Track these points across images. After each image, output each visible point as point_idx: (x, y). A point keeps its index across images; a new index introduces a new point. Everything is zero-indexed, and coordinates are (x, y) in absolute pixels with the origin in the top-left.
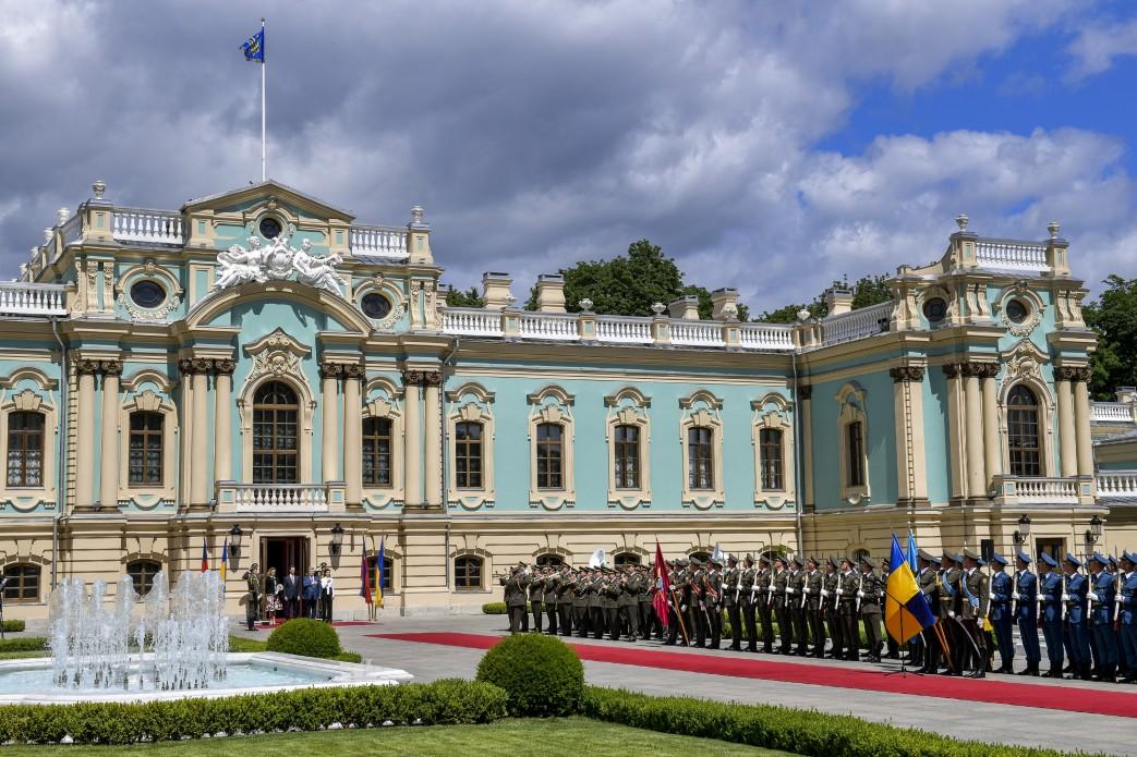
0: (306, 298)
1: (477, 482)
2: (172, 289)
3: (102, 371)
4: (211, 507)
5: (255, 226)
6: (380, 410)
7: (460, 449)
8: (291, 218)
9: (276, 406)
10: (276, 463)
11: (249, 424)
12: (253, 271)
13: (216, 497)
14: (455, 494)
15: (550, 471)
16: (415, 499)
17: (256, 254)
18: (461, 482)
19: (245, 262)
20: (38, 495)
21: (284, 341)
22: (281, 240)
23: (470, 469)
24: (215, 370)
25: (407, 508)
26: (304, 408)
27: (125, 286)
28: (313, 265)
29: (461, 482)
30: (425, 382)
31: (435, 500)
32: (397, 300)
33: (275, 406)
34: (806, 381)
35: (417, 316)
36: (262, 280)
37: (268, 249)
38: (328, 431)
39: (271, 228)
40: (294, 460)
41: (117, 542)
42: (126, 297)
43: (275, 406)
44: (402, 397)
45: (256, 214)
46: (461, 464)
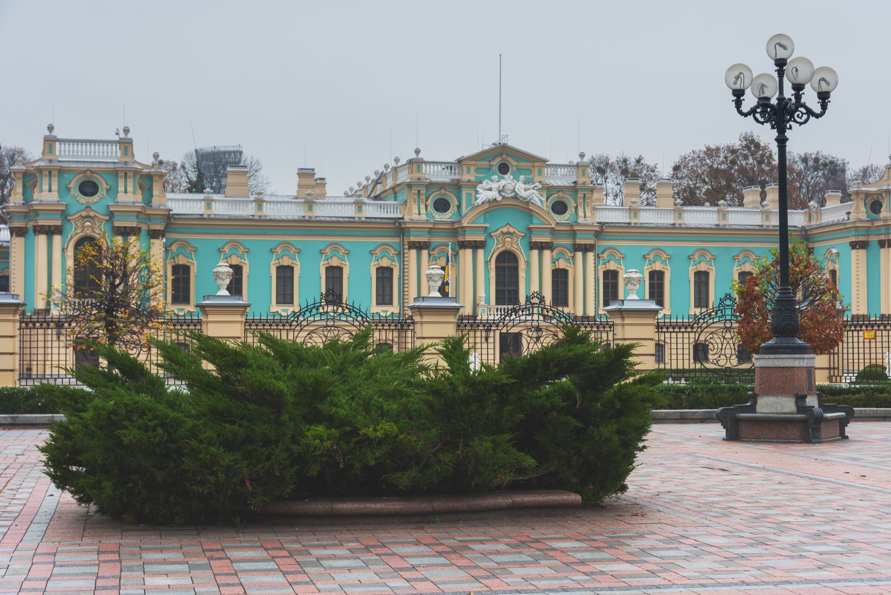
0: (524, 207)
2: (454, 202)
5: (495, 168)
6: (562, 264)
8: (516, 163)
11: (493, 274)
17: (495, 185)
19: (490, 189)
21: (511, 230)
22: (509, 177)
24: (476, 246)
26: (522, 265)
27: (430, 202)
28: (526, 190)
30: (586, 249)
32: (571, 205)
33: (506, 265)
35: (581, 214)
36: (499, 198)
37: (503, 182)
38: (535, 278)
39: (504, 169)
40: (516, 292)
42: (431, 209)
43: (506, 265)
44: (574, 257)
45: (496, 162)
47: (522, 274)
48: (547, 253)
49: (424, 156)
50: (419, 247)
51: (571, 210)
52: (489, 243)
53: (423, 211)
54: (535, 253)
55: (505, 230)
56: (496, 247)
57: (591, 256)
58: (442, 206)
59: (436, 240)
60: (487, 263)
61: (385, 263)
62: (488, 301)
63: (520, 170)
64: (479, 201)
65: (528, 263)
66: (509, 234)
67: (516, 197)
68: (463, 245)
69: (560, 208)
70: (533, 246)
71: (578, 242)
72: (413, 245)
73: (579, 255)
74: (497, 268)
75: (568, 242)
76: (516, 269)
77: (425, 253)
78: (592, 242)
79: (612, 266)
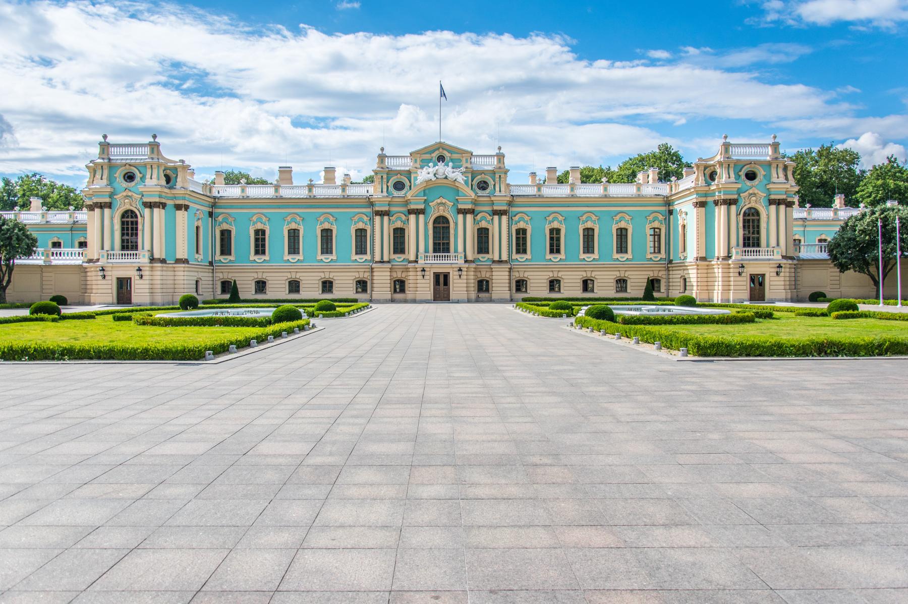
1: (525, 252)
3: (387, 213)
4: (416, 262)
5: (435, 159)
6: (484, 224)
7: (517, 238)
9: (441, 227)
10: (441, 245)
11: (431, 232)
12: (431, 176)
13: (417, 257)
14: (515, 256)
15: (555, 248)
16: (496, 258)
17: (430, 170)
18: (518, 252)
20: (365, 257)
23: (521, 247)
24: (417, 212)
25: (494, 262)
27: (391, 184)
29: (518, 252)
30: (500, 213)
31: (505, 257)
32: (491, 182)
34: (671, 208)
35: (497, 189)
36: (434, 179)
38: (463, 234)
40: (448, 244)
41: (389, 274)
45: (435, 155)
46: (518, 245)
47: (452, 231)
48: (469, 217)
49: (387, 152)
50: (381, 214)
51: (491, 187)
52: (428, 210)
53: (385, 190)
54: (461, 217)
55: (439, 201)
56: (433, 215)
57: (504, 218)
58: (399, 186)
59: (393, 209)
60: (426, 224)
61: (361, 226)
62: (426, 251)
63: (452, 160)
64: (418, 182)
65: (456, 224)
66: (441, 207)
67: (446, 178)
68: (410, 212)
69: (483, 186)
70: (460, 211)
71: (495, 208)
72: (378, 213)
73: (496, 218)
74: (434, 228)
75: (488, 209)
76: (449, 227)
77: (386, 218)
78: (505, 208)
79: (522, 225)
